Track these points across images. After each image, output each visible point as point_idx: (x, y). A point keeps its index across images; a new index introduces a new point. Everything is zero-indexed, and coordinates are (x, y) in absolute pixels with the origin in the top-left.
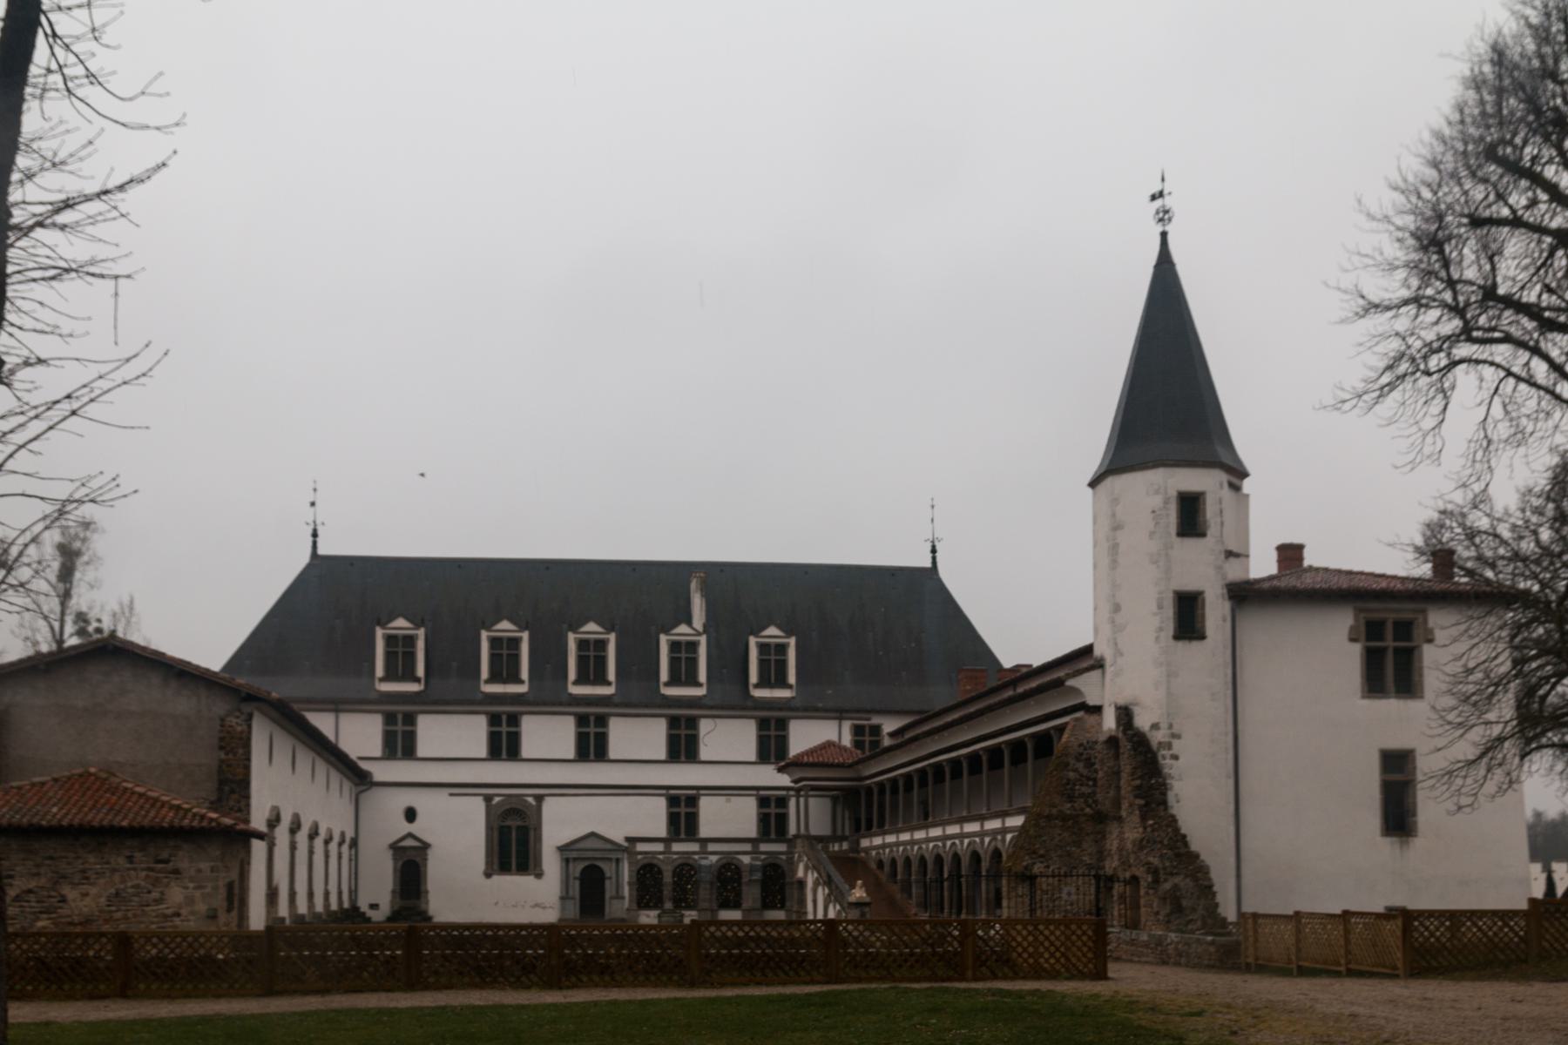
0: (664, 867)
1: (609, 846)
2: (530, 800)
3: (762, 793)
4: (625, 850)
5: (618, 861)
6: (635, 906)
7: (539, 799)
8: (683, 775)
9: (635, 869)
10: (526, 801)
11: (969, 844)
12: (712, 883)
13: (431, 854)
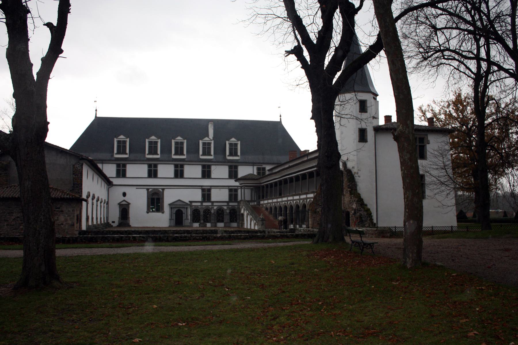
1: (184, 204)
2: (161, 190)
3: (230, 188)
5: (187, 208)
7: (163, 189)
8: (206, 183)
10: (159, 190)
11: (296, 202)
13: (131, 206)
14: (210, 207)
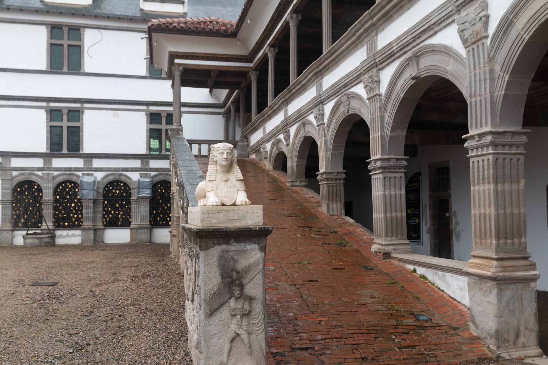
0: (43, 185)
3: (152, 108)
12: (95, 201)
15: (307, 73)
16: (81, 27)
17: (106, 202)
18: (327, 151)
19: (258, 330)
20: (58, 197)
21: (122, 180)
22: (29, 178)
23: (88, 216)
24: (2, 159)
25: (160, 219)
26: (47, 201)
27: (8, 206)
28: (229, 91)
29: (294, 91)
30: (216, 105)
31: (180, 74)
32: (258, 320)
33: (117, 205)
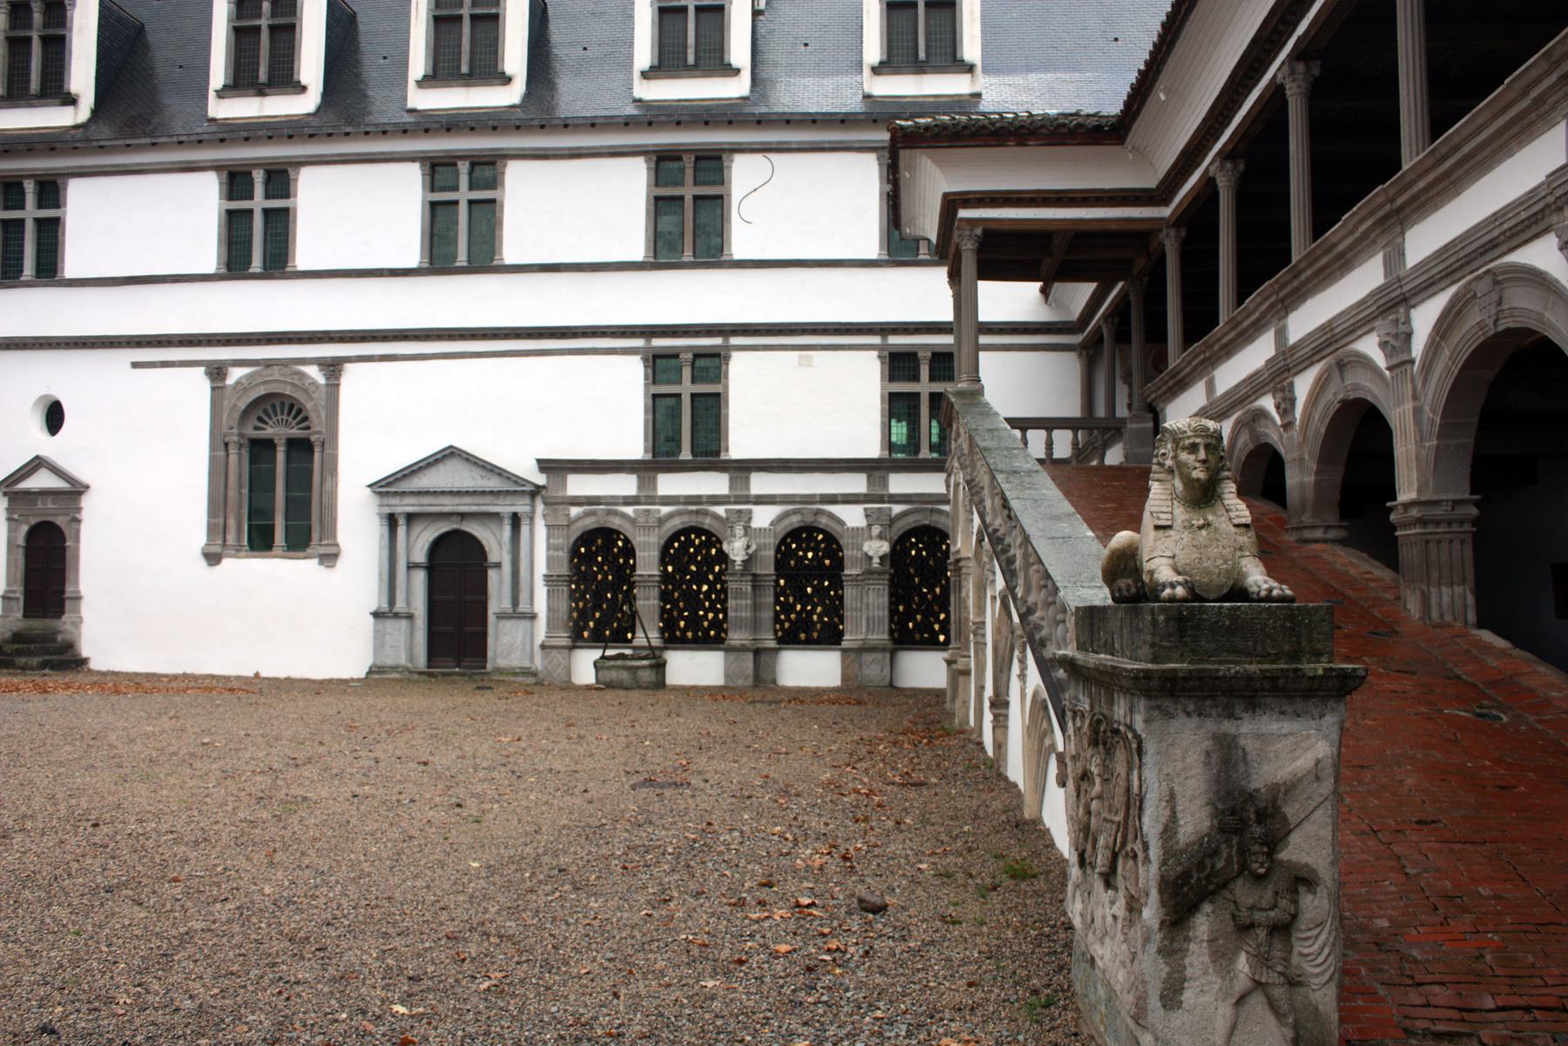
0: (638, 539)
1: (493, 483)
2: (313, 372)
3: (894, 340)
4: (536, 492)
5: (516, 520)
6: (563, 639)
7: (333, 368)
9: (565, 541)
10: (302, 375)
13: (86, 502)
14: (720, 510)
15: (1356, 220)
16: (724, 150)
17: (782, 582)
18: (1421, 440)
19: (1317, 975)
20: (670, 569)
21: (821, 526)
22: (606, 522)
23: (741, 617)
24: (548, 478)
25: (914, 625)
26: (646, 578)
27: (561, 588)
28: (1098, 287)
29: (1308, 273)
30: (1059, 326)
31: (975, 247)
32: (1316, 946)
33: (809, 590)
